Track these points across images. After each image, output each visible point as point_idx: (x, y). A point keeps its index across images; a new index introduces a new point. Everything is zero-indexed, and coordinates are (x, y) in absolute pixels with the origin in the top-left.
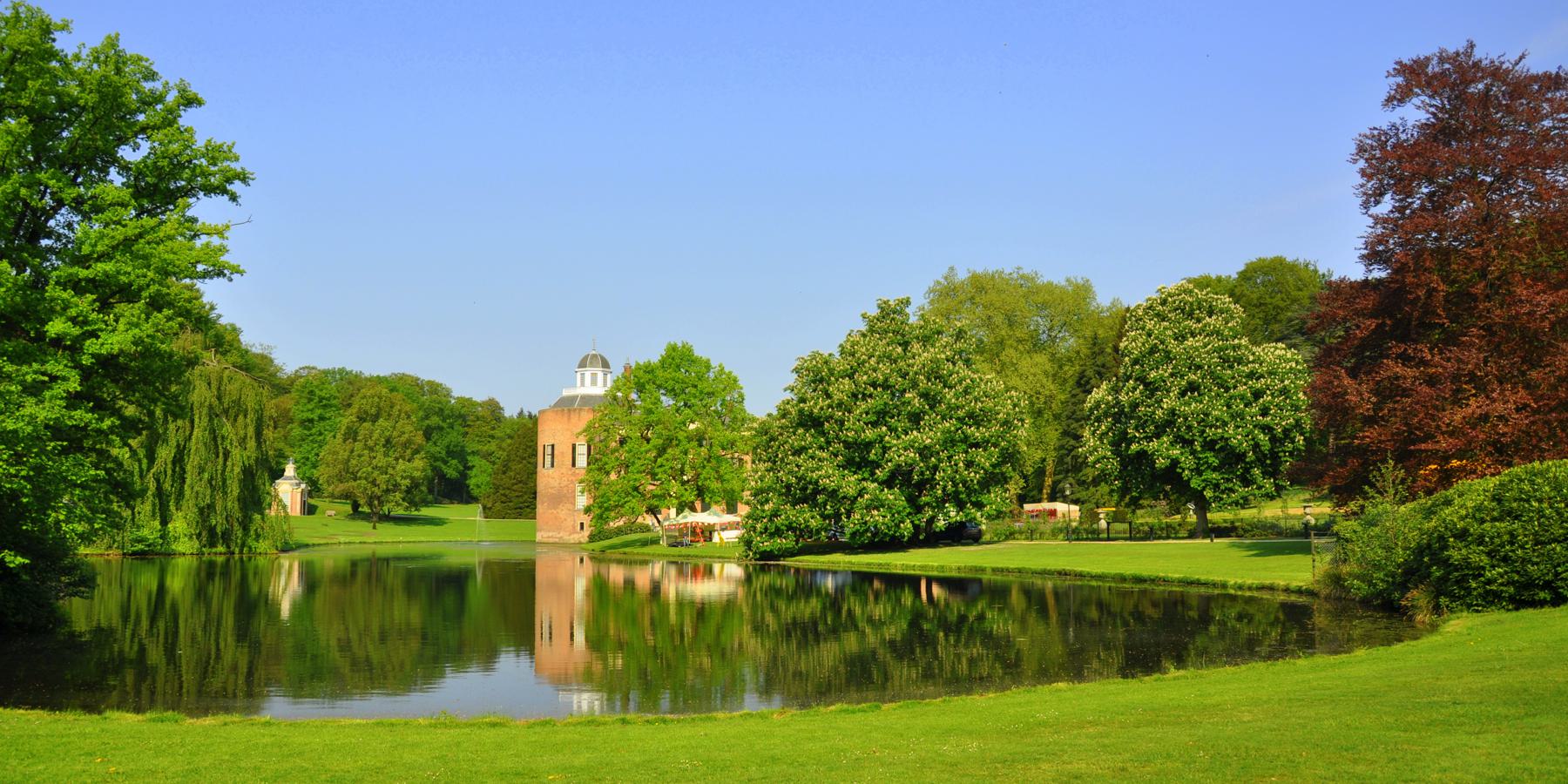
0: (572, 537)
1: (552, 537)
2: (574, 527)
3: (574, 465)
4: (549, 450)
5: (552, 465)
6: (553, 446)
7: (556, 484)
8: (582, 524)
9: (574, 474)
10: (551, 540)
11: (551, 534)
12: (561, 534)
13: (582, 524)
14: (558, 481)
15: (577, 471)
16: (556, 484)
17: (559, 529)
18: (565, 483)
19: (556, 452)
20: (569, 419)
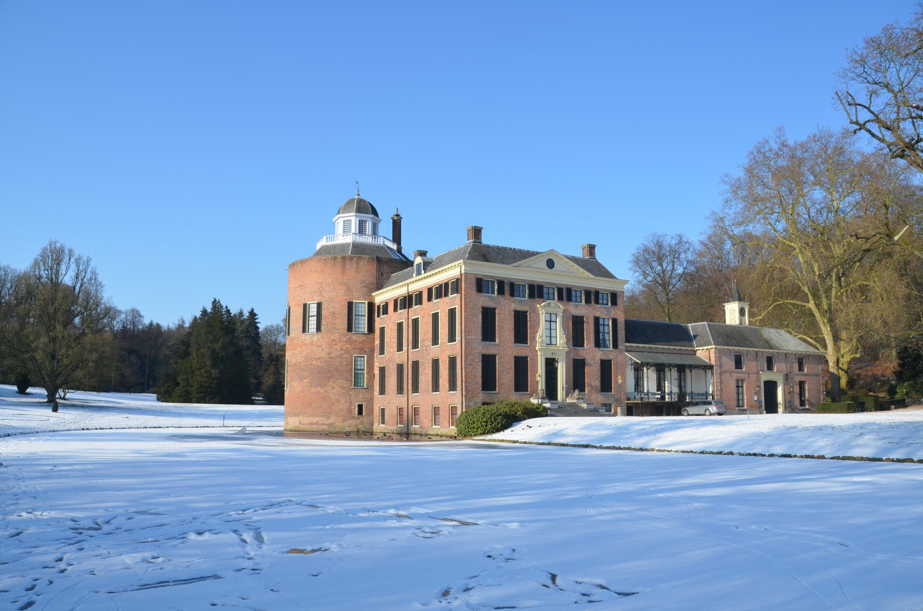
0: (347, 424)
1: (317, 423)
4: (313, 310)
5: (319, 329)
7: (324, 355)
8: (360, 407)
9: (350, 341)
10: (315, 428)
11: (315, 420)
12: (332, 420)
13: (360, 407)
14: (327, 350)
15: (354, 338)
16: (324, 355)
18: (338, 353)
19: (324, 312)
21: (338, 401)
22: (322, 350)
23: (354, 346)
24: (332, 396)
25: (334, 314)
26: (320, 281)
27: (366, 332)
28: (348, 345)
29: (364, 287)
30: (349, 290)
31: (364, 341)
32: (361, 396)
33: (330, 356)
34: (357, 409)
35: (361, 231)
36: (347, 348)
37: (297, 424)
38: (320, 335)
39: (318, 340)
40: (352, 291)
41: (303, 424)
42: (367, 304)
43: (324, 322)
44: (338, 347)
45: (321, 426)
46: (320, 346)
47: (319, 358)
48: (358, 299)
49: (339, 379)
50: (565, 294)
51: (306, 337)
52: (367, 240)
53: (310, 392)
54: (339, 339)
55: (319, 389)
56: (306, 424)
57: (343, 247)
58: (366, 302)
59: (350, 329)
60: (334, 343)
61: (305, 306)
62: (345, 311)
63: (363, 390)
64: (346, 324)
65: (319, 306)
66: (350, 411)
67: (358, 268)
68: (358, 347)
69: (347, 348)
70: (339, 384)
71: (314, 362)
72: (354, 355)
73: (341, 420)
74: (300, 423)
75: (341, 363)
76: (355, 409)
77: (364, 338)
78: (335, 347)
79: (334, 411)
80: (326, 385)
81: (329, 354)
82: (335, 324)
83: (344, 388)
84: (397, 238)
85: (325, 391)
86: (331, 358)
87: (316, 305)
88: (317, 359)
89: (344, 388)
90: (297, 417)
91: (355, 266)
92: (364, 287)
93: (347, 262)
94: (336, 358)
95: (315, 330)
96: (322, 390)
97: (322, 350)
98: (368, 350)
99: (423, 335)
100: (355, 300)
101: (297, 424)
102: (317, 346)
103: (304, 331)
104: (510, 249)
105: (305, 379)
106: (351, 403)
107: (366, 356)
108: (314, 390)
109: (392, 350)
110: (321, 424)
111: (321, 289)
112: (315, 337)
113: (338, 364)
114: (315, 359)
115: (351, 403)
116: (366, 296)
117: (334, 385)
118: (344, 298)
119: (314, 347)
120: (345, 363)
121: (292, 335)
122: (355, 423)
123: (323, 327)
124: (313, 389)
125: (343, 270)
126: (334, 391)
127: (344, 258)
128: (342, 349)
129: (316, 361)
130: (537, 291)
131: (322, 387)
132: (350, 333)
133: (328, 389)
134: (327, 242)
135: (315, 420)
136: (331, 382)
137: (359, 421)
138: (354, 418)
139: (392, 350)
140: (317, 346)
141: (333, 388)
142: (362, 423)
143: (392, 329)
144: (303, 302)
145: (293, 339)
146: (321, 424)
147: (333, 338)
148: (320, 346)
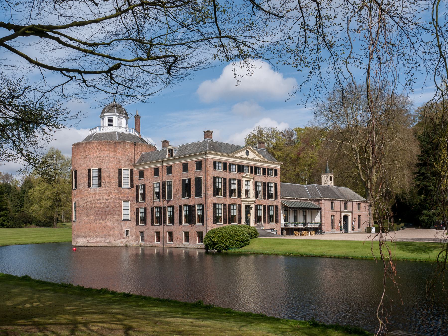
1: (100, 242)
2: (121, 234)
3: (120, 185)
4: (95, 173)
5: (100, 185)
6: (100, 170)
7: (104, 200)
8: (127, 231)
9: (120, 193)
11: (99, 240)
12: (110, 239)
13: (127, 231)
14: (106, 198)
15: (123, 190)
16: (104, 200)
17: (107, 235)
18: (113, 200)
20: (115, 150)
21: (114, 228)
22: (103, 197)
23: (123, 196)
24: (110, 225)
25: (110, 176)
26: (100, 155)
27: (130, 187)
28: (119, 195)
29: (128, 160)
30: (119, 161)
31: (128, 192)
32: (127, 225)
33: (108, 201)
34: (125, 233)
35: (120, 125)
36: (119, 197)
37: (86, 242)
38: (100, 189)
39: (100, 191)
40: (121, 162)
41: (90, 243)
42: (130, 170)
43: (103, 181)
44: (113, 196)
45: (103, 243)
46: (101, 195)
47: (101, 203)
48: (124, 167)
49: (114, 215)
50: (254, 170)
51: (91, 190)
52: (122, 130)
53: (95, 223)
54: (113, 191)
55: (101, 221)
56: (92, 242)
57: (112, 135)
58: (130, 169)
59: (120, 185)
60: (111, 193)
61: (90, 170)
62: (117, 174)
63: (129, 222)
64: (118, 182)
65: (100, 170)
66: (121, 234)
67: (124, 149)
68: (125, 196)
69: (119, 197)
70: (114, 218)
71: (97, 205)
72: (123, 201)
73: (116, 239)
74: (88, 242)
75: (115, 205)
76: (124, 233)
77: (127, 191)
78: (111, 196)
79: (112, 234)
80: (106, 219)
81: (107, 200)
82: (110, 182)
83: (117, 220)
84: (138, 129)
85: (106, 223)
86: (109, 202)
87: (97, 171)
88: (99, 203)
89: (117, 220)
90: (85, 239)
91: (122, 147)
92: (128, 160)
93: (117, 145)
94: (112, 202)
95: (97, 186)
96: (103, 222)
97: (103, 197)
98: (131, 198)
99: (175, 191)
100: (123, 168)
101: (86, 242)
102: (99, 195)
103: (89, 186)
104: (226, 144)
105: (91, 215)
106: (122, 229)
107: (130, 201)
108: (98, 222)
109: (149, 199)
110: (103, 242)
111: (101, 161)
112: (98, 190)
113: (113, 206)
114: (98, 203)
115: (122, 229)
116: (129, 166)
117: (111, 219)
118: (116, 166)
119: (97, 196)
120: (117, 206)
121: (80, 188)
122: (125, 241)
123: (102, 184)
124: (97, 221)
125: (115, 150)
126: (112, 222)
127: (115, 143)
128: (115, 198)
129: (99, 204)
130: (241, 168)
131: (103, 220)
132: (120, 188)
133: (107, 221)
134: (99, 130)
135: (99, 240)
136: (109, 217)
137: (126, 240)
138: (124, 238)
139: (149, 199)
140: (99, 195)
141: (111, 221)
142: (128, 241)
143: (149, 186)
144: (88, 168)
145: (80, 191)
146: (103, 242)
147: (109, 190)
148: (101, 195)
